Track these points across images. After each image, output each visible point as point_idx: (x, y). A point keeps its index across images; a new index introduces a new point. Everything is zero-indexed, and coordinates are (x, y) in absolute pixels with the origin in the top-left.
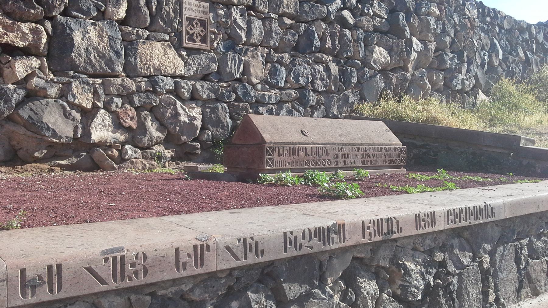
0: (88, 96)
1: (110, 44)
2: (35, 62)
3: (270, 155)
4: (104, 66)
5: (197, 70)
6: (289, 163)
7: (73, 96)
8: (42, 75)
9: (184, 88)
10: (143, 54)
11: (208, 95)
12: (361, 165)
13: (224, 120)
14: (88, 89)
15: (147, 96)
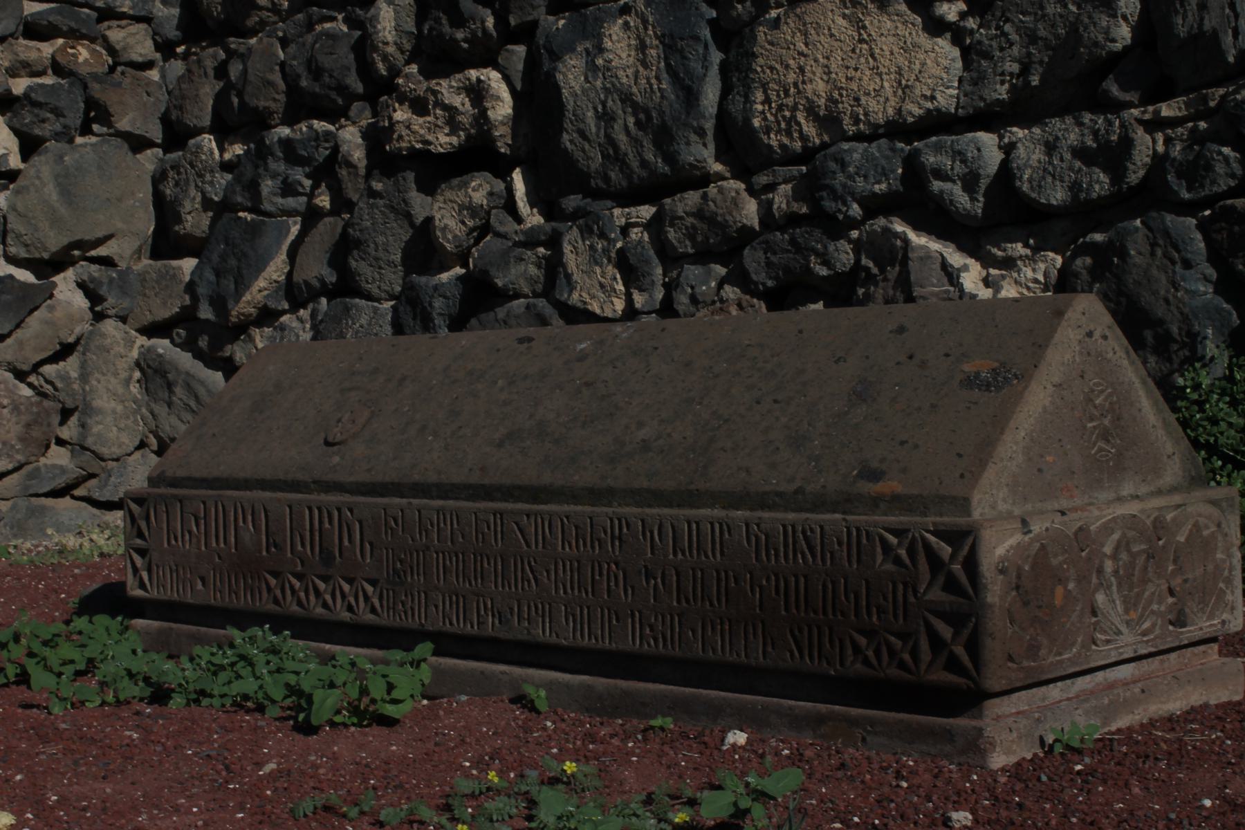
0: (603, 274)
1: (668, 65)
2: (479, 189)
3: (140, 535)
4: (650, 156)
5: (1025, 70)
6: (203, 579)
7: (568, 277)
8: (510, 226)
9: (940, 175)
10: (772, 68)
11: (1075, 187)
12: (568, 635)
13: (1160, 311)
14: (603, 250)
15: (793, 241)
